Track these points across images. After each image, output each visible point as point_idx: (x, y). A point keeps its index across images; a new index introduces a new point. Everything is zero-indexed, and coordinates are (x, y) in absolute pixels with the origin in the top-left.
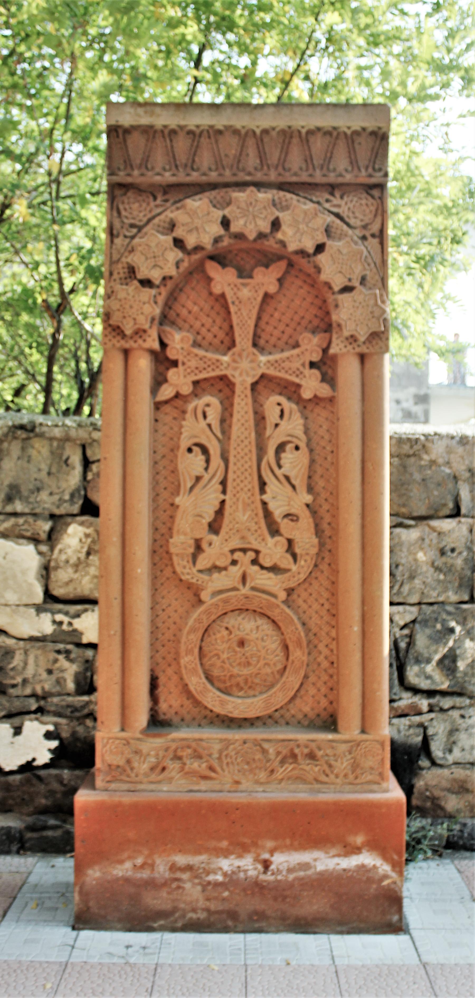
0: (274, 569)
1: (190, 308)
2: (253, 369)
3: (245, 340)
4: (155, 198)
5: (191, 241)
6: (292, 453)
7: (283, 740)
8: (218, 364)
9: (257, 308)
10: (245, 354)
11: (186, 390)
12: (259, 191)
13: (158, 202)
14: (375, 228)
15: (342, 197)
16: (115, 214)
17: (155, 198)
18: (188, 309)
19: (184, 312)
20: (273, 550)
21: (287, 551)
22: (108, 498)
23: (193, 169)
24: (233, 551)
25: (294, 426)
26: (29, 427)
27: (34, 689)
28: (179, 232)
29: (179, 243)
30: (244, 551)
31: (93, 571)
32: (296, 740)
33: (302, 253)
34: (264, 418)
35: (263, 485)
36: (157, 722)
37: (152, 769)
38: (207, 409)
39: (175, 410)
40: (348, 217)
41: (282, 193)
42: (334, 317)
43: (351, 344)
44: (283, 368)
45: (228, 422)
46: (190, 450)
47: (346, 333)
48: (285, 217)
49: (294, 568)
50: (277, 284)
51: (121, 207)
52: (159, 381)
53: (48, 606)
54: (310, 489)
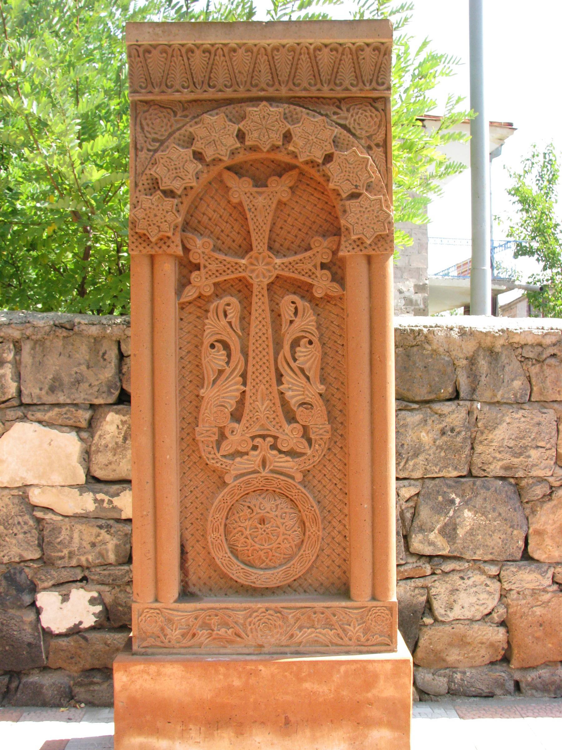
0: (292, 453)
1: (211, 216)
2: (269, 271)
3: (261, 244)
4: (175, 115)
5: (209, 154)
6: (306, 347)
7: (302, 608)
8: (237, 266)
9: (272, 214)
10: (261, 257)
11: (208, 291)
12: (271, 105)
13: (178, 118)
14: (379, 138)
15: (348, 110)
16: (139, 130)
17: (175, 115)
18: (208, 216)
19: (205, 219)
20: (290, 436)
21: (303, 437)
22: (139, 389)
24: (253, 438)
25: (307, 321)
26: (68, 326)
27: (79, 560)
28: (198, 146)
29: (198, 156)
30: (264, 437)
31: (129, 453)
32: (313, 608)
33: (312, 163)
34: (279, 315)
35: (280, 376)
36: (186, 594)
37: (184, 635)
38: (227, 308)
39: (199, 310)
40: (354, 128)
41: (292, 107)
42: (343, 222)
43: (358, 246)
44: (296, 269)
45: (247, 320)
46: (212, 346)
47: (354, 237)
49: (309, 452)
50: (289, 190)
51: (144, 123)
52: (183, 283)
53: (90, 486)
54: (323, 380)
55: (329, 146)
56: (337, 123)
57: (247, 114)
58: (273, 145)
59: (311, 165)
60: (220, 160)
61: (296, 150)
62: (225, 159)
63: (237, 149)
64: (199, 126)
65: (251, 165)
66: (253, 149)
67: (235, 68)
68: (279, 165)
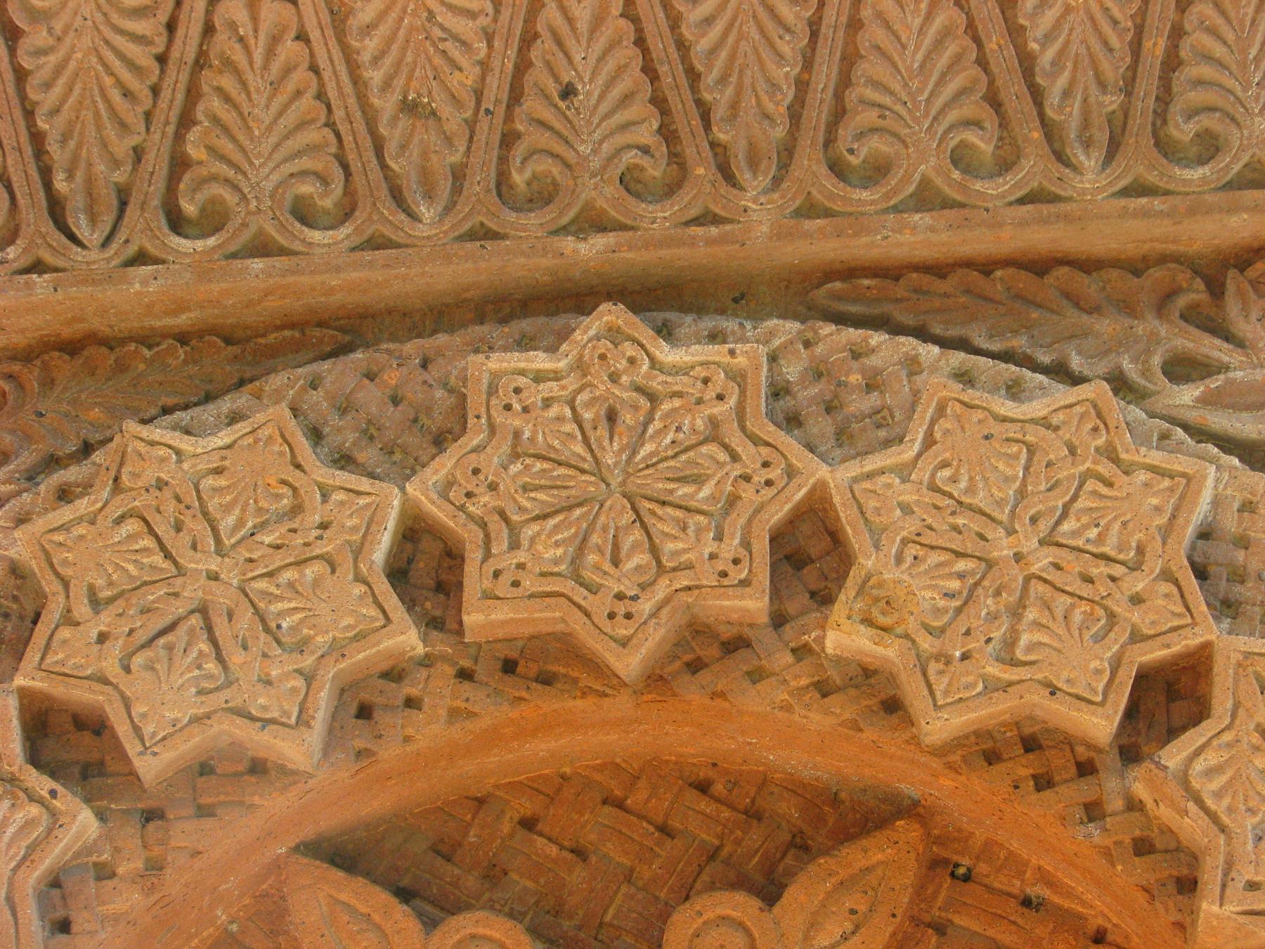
12: (665, 332)
23: (177, 223)
33: (1029, 751)
41: (834, 338)
48: (874, 490)
55: (1163, 601)
56: (1200, 434)
57: (475, 402)
58: (697, 630)
59: (1024, 768)
60: (258, 768)
61: (889, 652)
62: (298, 749)
63: (393, 675)
64: (83, 506)
65: (528, 824)
66: (535, 665)
67: (375, 76)
68: (754, 814)
